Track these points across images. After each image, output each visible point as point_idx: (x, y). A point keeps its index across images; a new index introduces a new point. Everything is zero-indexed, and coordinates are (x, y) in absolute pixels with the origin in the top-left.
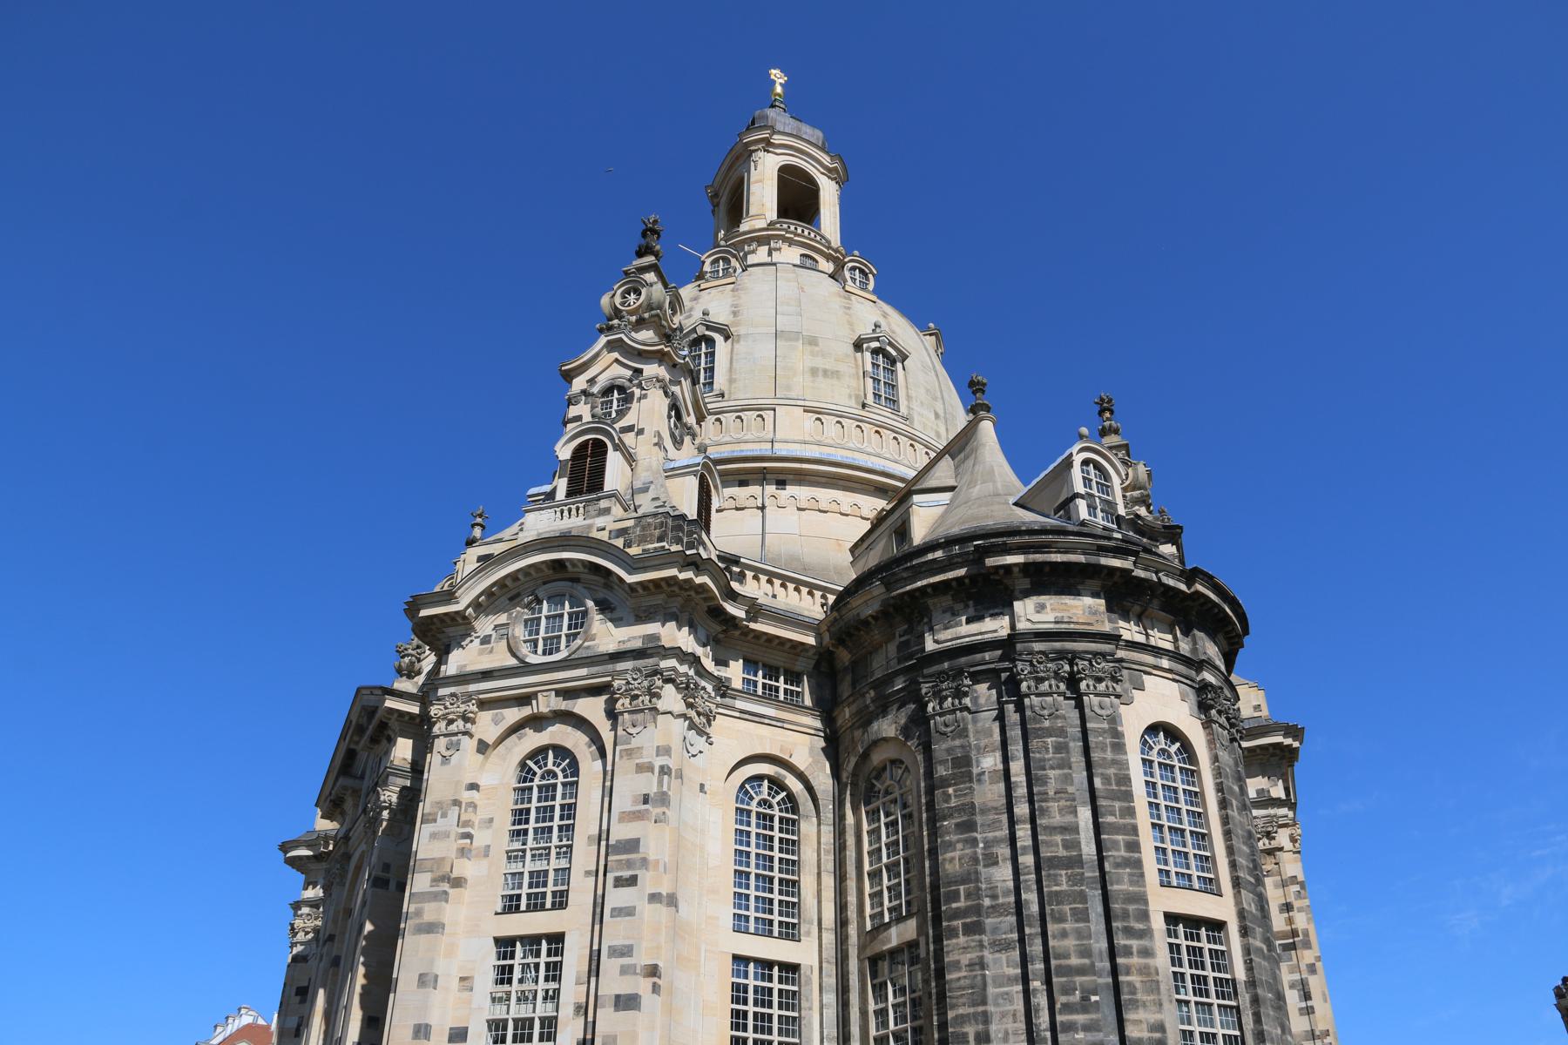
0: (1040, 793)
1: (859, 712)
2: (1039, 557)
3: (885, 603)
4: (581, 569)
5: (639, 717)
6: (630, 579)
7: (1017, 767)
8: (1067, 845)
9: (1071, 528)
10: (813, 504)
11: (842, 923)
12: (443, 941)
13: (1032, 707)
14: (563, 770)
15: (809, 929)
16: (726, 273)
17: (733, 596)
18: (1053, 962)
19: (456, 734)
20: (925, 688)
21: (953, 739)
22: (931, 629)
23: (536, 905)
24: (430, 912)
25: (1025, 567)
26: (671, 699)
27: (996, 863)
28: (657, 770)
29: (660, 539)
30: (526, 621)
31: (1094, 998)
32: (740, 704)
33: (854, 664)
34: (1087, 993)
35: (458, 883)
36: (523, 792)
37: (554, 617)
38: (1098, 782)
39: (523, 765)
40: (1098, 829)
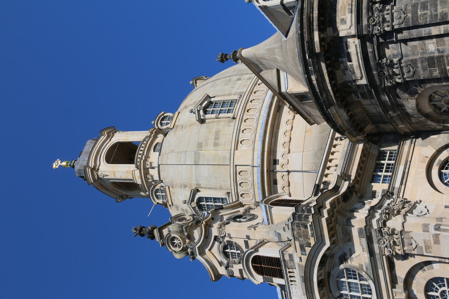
1: (401, 119)
2: (315, 23)
3: (340, 107)
4: (323, 271)
5: (406, 241)
6: (328, 244)
7: (435, 31)
9: (299, 6)
10: (286, 145)
13: (399, 24)
14: (440, 286)
16: (164, 191)
17: (336, 188)
20: (388, 84)
21: (417, 67)
22: (355, 81)
25: (321, 30)
26: (395, 223)
29: (306, 227)
32: (397, 185)
33: (374, 122)
37: (350, 287)
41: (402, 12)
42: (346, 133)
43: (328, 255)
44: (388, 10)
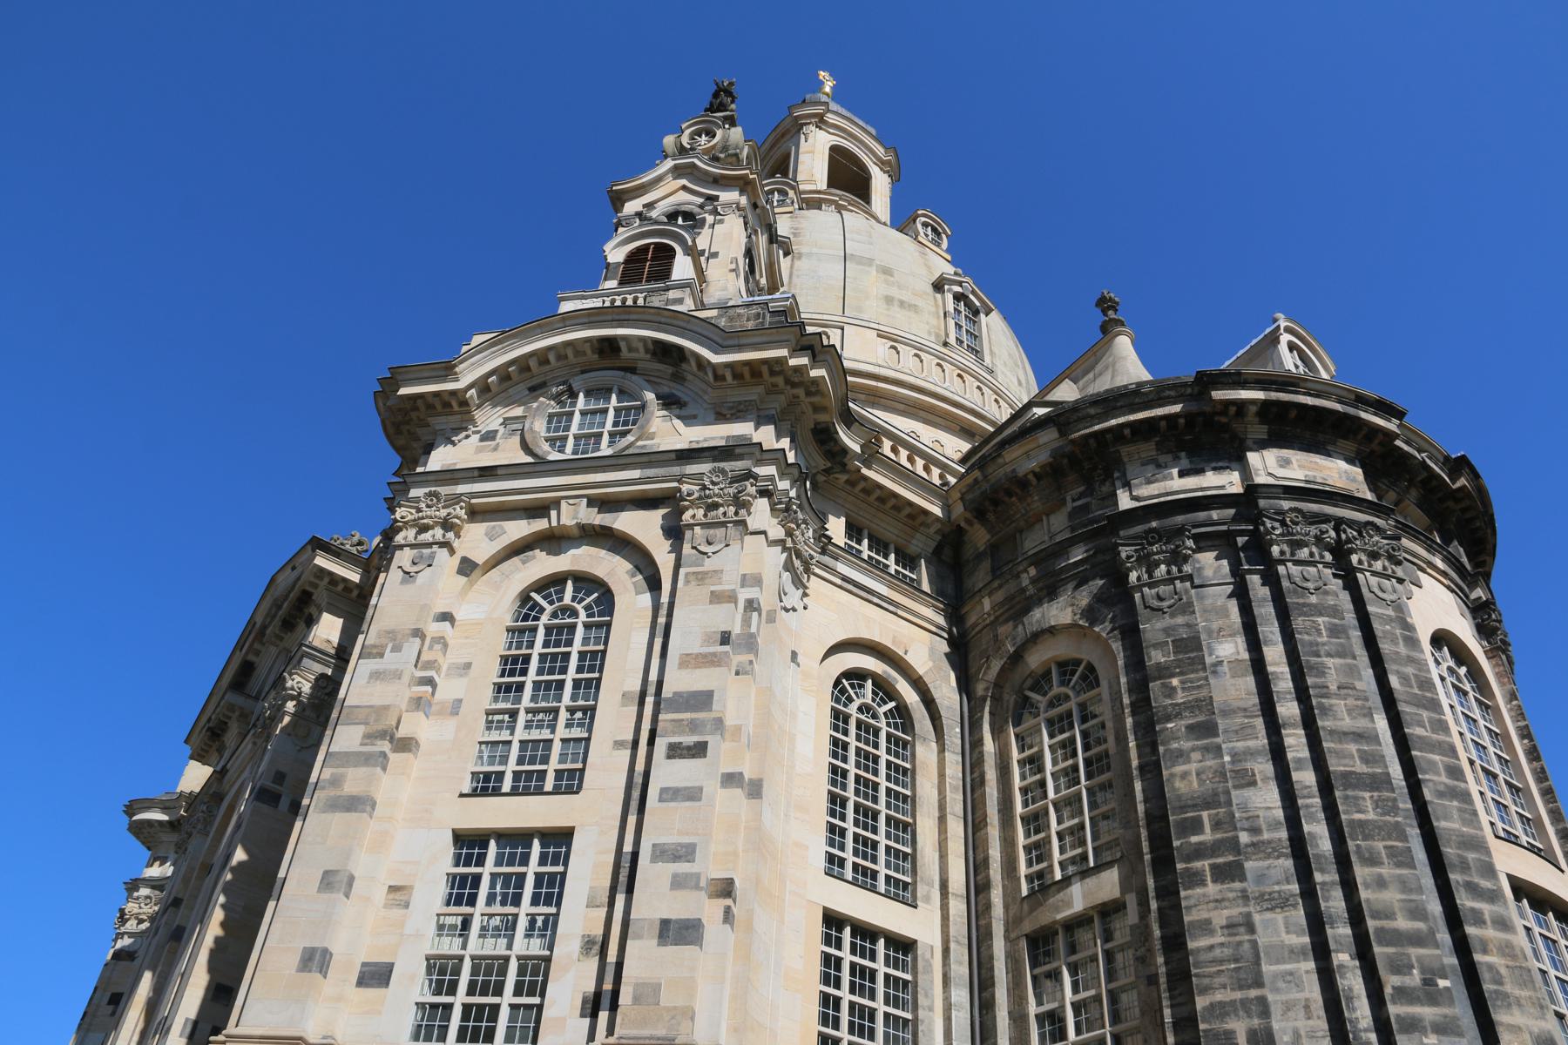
1: (1009, 598)
3: (1055, 454)
4: (642, 354)
5: (720, 532)
7: (1274, 654)
8: (1367, 758)
11: (978, 887)
12: (370, 826)
14: (587, 608)
15: (928, 890)
17: (849, 419)
18: (1371, 924)
19: (429, 545)
20: (1124, 552)
21: (1173, 616)
22: (1127, 485)
23: (528, 784)
24: (354, 781)
25: (1266, 405)
27: (1253, 783)
28: (741, 605)
30: (551, 416)
32: (842, 568)
33: (994, 549)
35: (406, 745)
36: (520, 633)
37: (594, 412)
38: (1394, 681)
39: (525, 598)
41: (1320, 583)
42: (977, 474)
43: (684, 366)
44: (1322, 557)
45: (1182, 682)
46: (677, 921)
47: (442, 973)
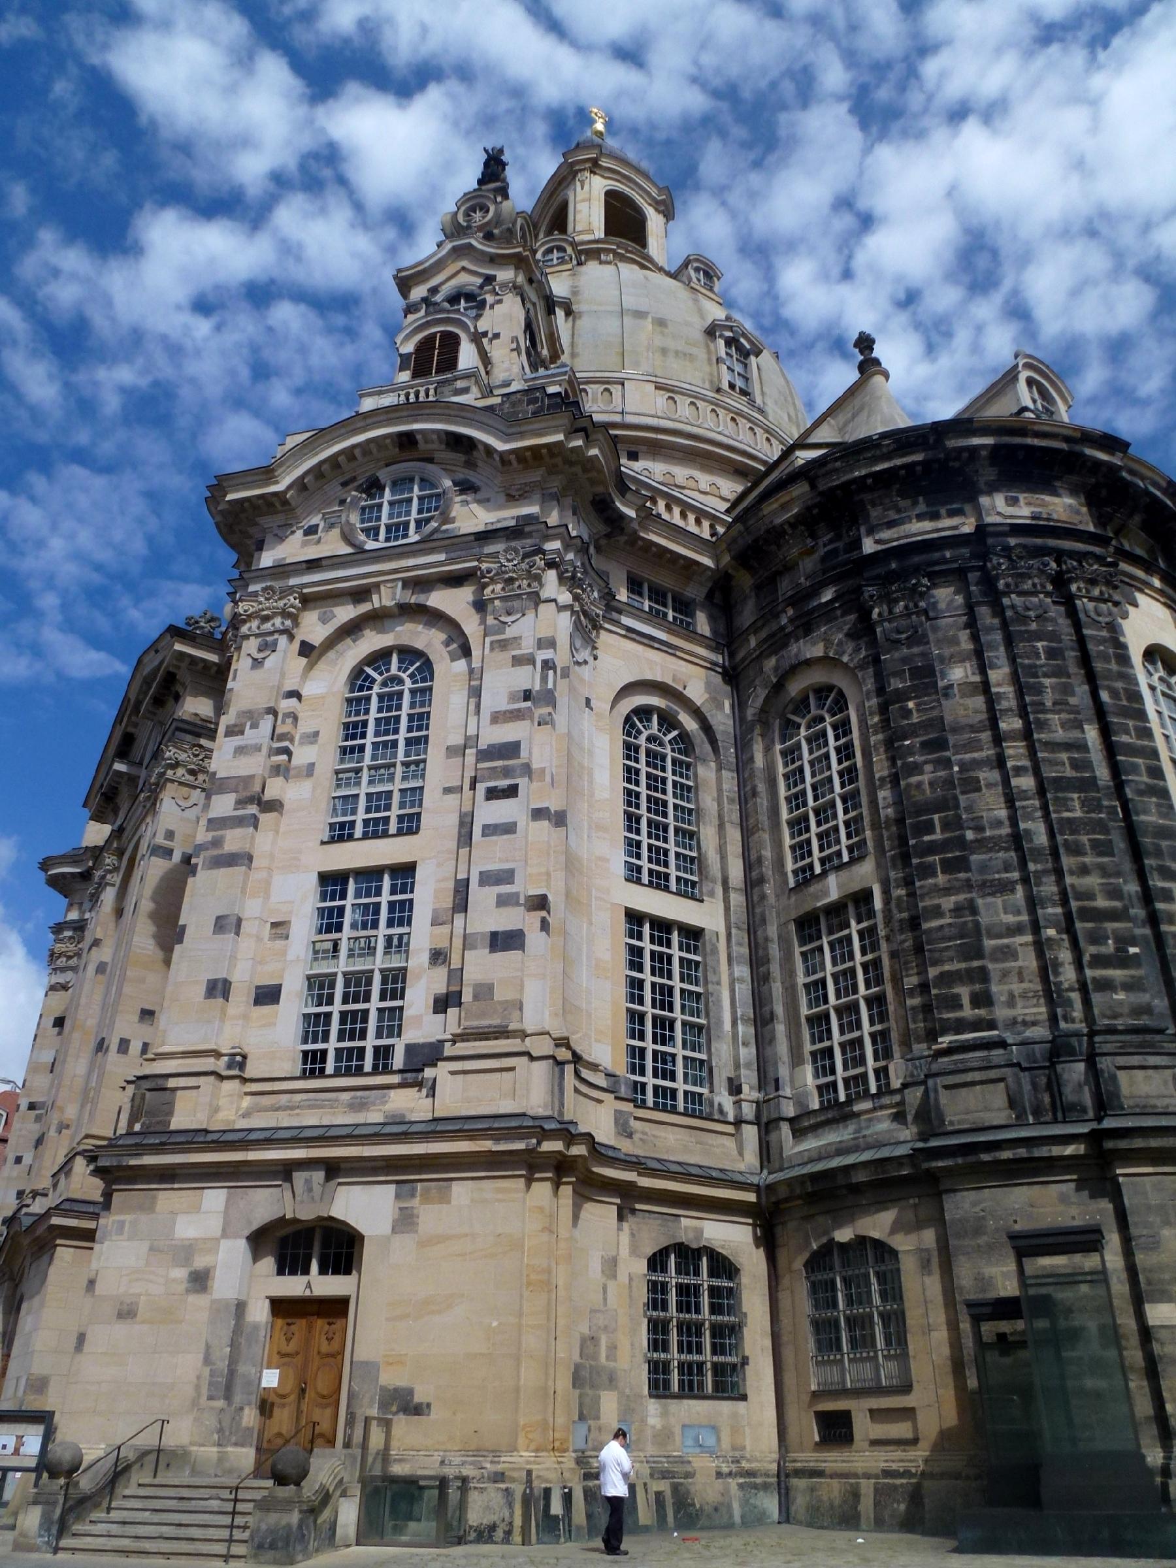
0: (1033, 704)
1: (771, 636)
5: (516, 604)
8: (1075, 765)
11: (753, 883)
13: (1013, 607)
14: (411, 676)
18: (1074, 904)
19: (272, 633)
23: (376, 830)
27: (979, 789)
30: (363, 509)
31: (1133, 950)
34: (1123, 941)
35: (274, 806)
36: (357, 704)
37: (400, 502)
38: (1105, 696)
40: (1111, 749)
41: (1040, 611)
42: (739, 526)
44: (1043, 586)
45: (917, 705)
46: (504, 933)
47: (320, 987)
